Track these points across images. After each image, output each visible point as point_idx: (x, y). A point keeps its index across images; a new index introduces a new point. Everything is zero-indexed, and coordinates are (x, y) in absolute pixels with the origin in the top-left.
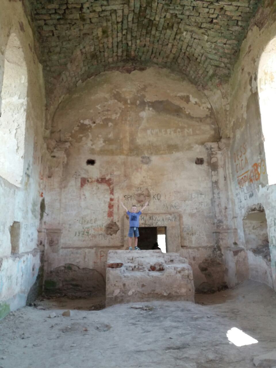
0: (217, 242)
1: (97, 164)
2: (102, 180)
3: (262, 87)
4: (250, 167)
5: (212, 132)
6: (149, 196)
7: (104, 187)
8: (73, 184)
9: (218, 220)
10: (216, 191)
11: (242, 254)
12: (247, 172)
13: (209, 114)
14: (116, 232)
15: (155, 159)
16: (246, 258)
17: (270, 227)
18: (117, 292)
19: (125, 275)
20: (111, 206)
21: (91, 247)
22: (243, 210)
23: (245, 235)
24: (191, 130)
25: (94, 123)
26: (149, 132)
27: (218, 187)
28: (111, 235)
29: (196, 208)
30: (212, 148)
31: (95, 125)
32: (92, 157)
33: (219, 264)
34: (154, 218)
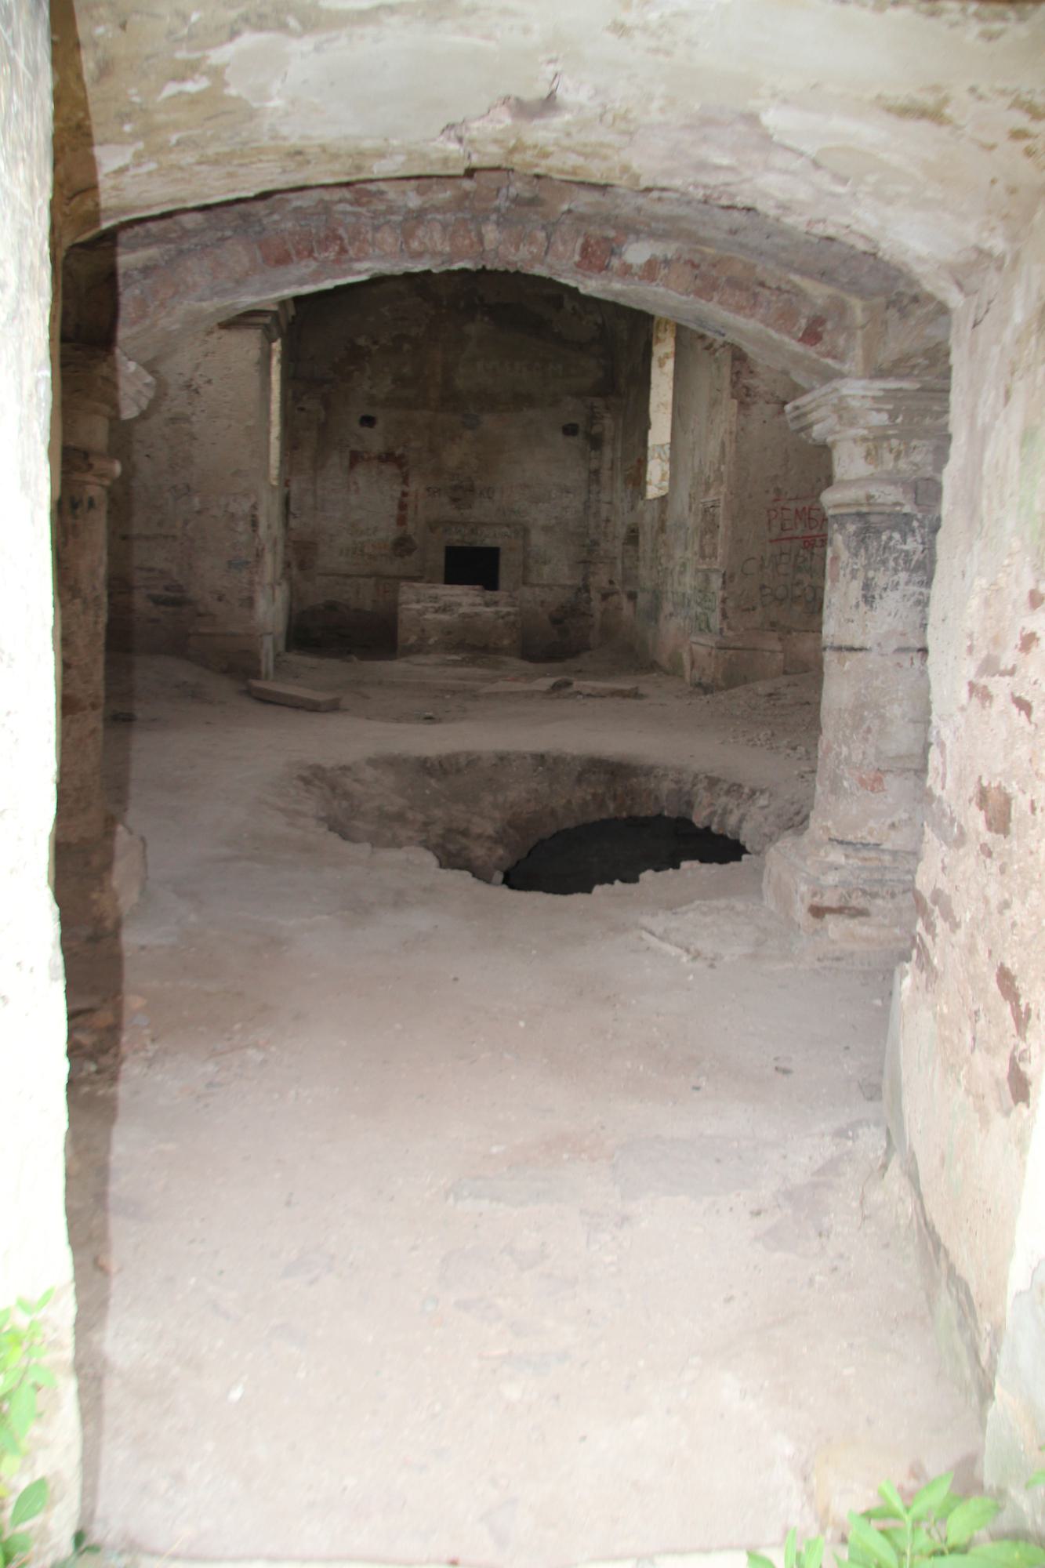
0: (585, 578)
1: (380, 425)
2: (388, 457)
3: (660, 335)
6: (472, 489)
7: (390, 469)
8: (336, 461)
9: (591, 541)
10: (594, 488)
11: (614, 599)
14: (410, 552)
15: (488, 421)
16: (619, 608)
18: (413, 639)
19: (426, 617)
20: (402, 506)
21: (369, 576)
25: (375, 343)
27: (598, 482)
28: (402, 556)
29: (556, 518)
30: (595, 407)
31: (377, 347)
32: (369, 412)
33: (584, 614)
34: (479, 532)
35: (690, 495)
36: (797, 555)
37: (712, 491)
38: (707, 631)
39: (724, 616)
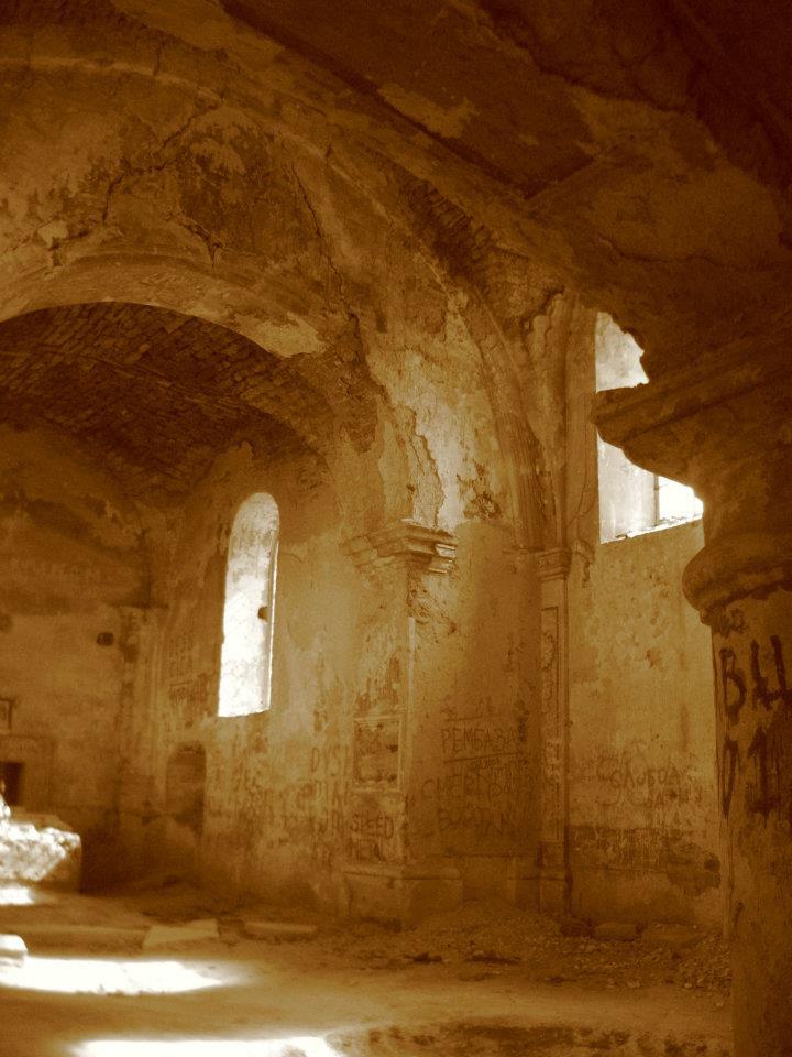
3: (235, 551)
4: (195, 676)
5: (137, 584)
12: (188, 682)
13: (136, 544)
17: (211, 781)
22: (171, 746)
23: (167, 788)
24: (97, 572)
26: (14, 562)
27: (131, 695)
35: (316, 714)
36: (466, 777)
37: (376, 710)
38: (375, 858)
39: (407, 843)
